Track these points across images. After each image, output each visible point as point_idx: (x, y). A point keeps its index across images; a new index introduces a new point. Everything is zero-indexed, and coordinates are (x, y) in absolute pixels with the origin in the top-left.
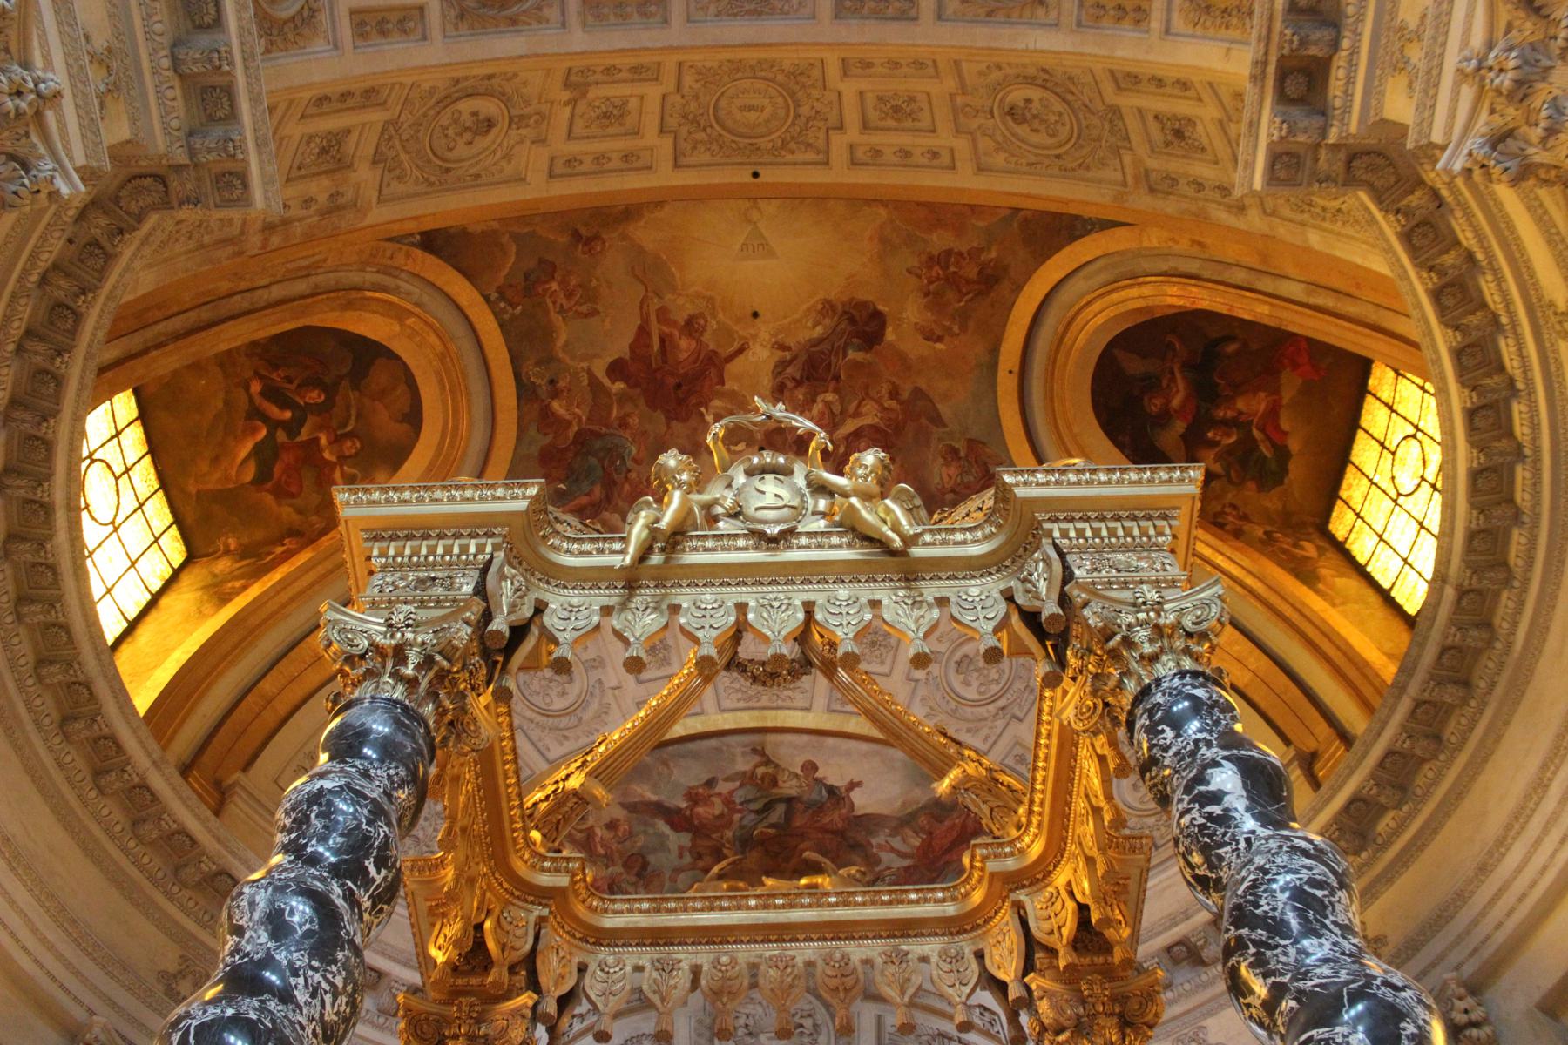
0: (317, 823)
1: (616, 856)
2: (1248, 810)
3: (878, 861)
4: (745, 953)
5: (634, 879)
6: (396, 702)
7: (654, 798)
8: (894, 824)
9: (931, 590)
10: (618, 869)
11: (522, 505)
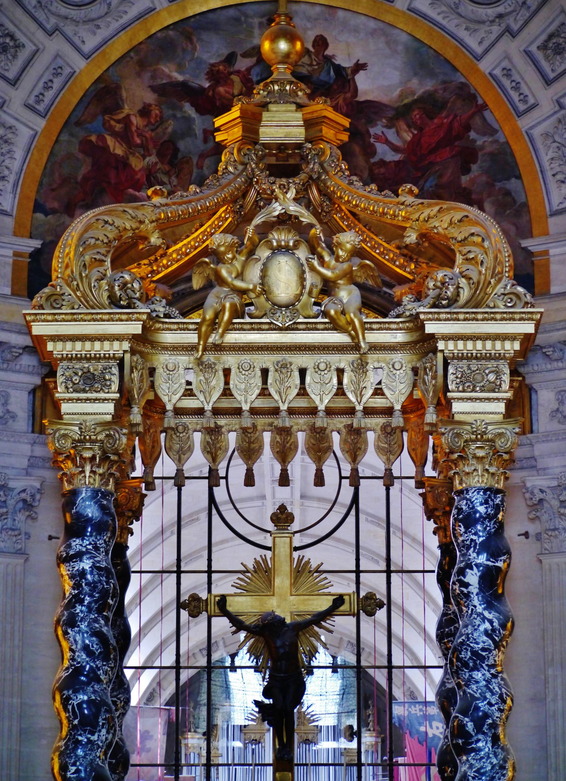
0: (86, 589)
1: (151, 146)
2: (477, 594)
3: (374, 152)
4: (261, 421)
5: (167, 168)
6: (95, 492)
7: (180, 78)
8: (391, 114)
9: (373, 359)
10: (152, 159)
11: (136, 328)
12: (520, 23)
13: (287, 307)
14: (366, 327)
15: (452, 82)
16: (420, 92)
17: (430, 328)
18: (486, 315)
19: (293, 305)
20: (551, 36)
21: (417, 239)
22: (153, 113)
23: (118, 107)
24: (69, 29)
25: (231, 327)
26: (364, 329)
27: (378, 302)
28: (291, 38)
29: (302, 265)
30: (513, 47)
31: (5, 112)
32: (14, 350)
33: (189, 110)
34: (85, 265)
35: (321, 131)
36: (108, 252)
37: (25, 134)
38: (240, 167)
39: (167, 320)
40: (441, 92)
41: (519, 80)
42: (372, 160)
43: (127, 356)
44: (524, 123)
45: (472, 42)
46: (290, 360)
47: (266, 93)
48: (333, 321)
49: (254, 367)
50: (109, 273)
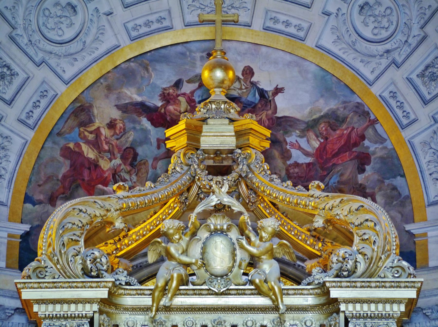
1: (116, 151)
3: (289, 157)
5: (129, 168)
8: (303, 126)
10: (118, 161)
11: (103, 294)
12: (403, 57)
13: (222, 277)
14: (284, 293)
15: (350, 102)
16: (325, 110)
17: (334, 293)
18: (378, 284)
19: (227, 275)
20: (427, 67)
21: (323, 224)
22: (118, 126)
23: (91, 121)
24: (53, 62)
25: (178, 292)
26: (282, 294)
27: (293, 274)
28: (226, 68)
29: (234, 244)
30: (397, 76)
31: (2, 125)
32: (8, 311)
33: (146, 123)
34: (63, 244)
35: (248, 140)
36: (82, 234)
37: (18, 142)
38: (186, 168)
39: (128, 287)
40: (342, 110)
41: (404, 101)
42: (288, 163)
43: (96, 316)
44: (407, 134)
45: (366, 71)
46: (224, 318)
47: (205, 111)
48: (257, 288)
49: (196, 324)
50: (83, 250)
